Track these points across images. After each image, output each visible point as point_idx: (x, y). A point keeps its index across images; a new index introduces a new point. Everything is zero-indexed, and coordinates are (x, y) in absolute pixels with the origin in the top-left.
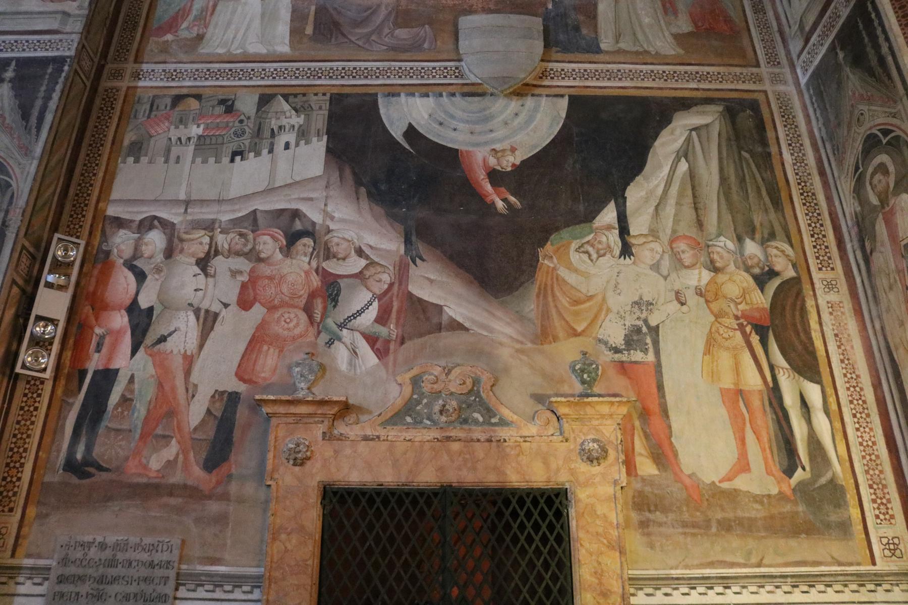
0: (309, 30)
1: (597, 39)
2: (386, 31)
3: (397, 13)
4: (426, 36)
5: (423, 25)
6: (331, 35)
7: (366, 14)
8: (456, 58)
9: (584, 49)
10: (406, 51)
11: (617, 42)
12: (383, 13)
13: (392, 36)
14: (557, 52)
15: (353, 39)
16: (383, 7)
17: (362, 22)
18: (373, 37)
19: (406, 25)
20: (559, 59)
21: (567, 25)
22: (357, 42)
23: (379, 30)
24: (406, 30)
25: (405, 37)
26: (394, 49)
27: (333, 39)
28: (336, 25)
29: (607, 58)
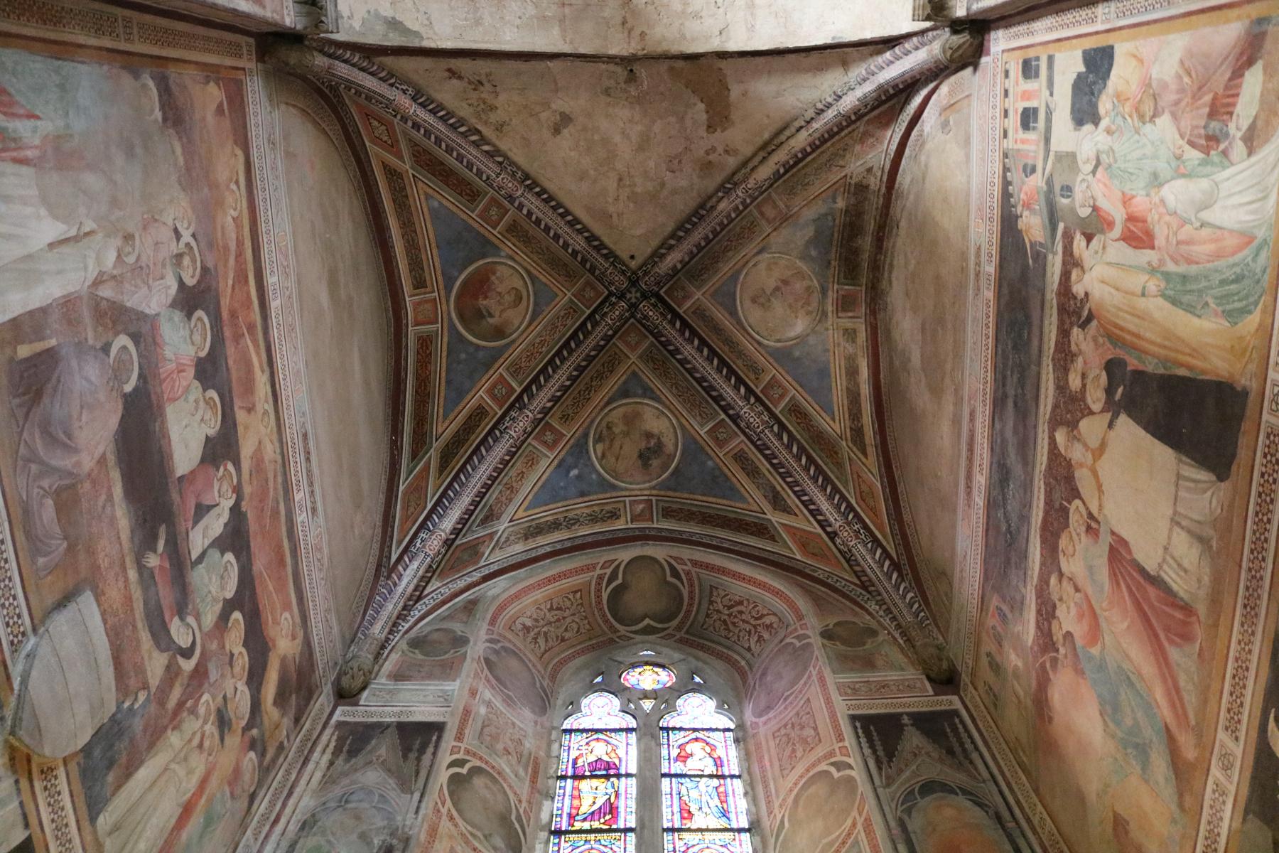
0: (24, 351)
1: (107, 801)
2: (45, 483)
3: (73, 485)
4: (53, 552)
5: (66, 538)
6: (24, 394)
7: (62, 436)
8: (36, 621)
9: (91, 797)
10: (28, 534)
11: (110, 834)
12: (65, 462)
13: (44, 496)
14: (78, 764)
15: (25, 435)
16: (74, 459)
17: (51, 435)
18: (34, 468)
19: (59, 509)
20: (71, 776)
21: (112, 746)
22: (22, 443)
23: (48, 470)
24: (54, 514)
25: (45, 521)
26: (27, 511)
27: (17, 401)
28: (38, 395)
29: (88, 838)
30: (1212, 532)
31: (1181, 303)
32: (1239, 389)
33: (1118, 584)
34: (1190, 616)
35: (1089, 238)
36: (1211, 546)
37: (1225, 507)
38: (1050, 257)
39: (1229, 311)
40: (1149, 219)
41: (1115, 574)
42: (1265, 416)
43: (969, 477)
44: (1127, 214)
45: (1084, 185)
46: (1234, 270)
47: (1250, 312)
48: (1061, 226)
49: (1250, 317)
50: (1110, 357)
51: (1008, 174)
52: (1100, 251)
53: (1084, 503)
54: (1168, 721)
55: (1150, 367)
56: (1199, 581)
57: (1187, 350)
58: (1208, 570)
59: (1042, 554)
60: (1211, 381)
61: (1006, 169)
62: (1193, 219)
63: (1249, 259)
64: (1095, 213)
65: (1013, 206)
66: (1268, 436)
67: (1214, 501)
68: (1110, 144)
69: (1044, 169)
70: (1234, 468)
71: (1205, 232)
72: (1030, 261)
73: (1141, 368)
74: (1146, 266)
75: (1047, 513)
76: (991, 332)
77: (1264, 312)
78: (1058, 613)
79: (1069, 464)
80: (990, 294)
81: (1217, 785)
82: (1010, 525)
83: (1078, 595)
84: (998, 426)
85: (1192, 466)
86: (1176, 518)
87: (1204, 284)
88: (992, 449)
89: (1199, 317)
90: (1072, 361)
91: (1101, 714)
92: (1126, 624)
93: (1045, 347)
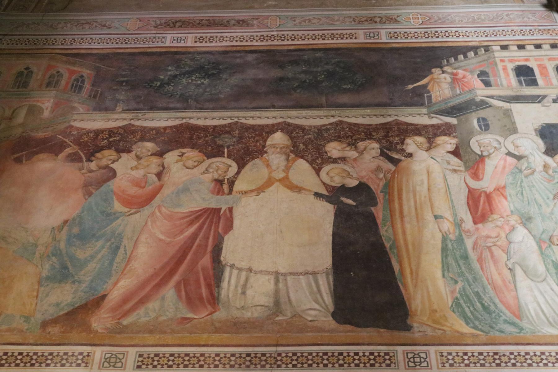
30: (289, 314)
31: (446, 256)
32: (409, 322)
33: (191, 223)
34: (210, 304)
35: (456, 153)
36: (278, 316)
37: (315, 324)
38: (424, 110)
39: (459, 303)
40: (495, 216)
41: (197, 218)
42: (400, 349)
43: (185, 24)
44: (491, 193)
45: (495, 144)
46: (491, 304)
47: (467, 324)
48: (453, 121)
49: (463, 323)
50: (372, 187)
51: (472, 53)
52: (451, 167)
53: (238, 173)
54: (109, 297)
55: (385, 232)
56: (243, 308)
57: (414, 268)
58: (256, 315)
59: (165, 128)
60: (401, 295)
61: (475, 49)
62: (512, 261)
63: (504, 317)
64: (478, 158)
65: (448, 61)
66: (387, 354)
67: (313, 313)
68: (537, 170)
69: (492, 97)
70: (348, 327)
71: (507, 273)
72: (410, 87)
73: (379, 221)
74: (459, 218)
75: (205, 129)
76: (329, 42)
77: (473, 335)
78: (124, 156)
79: (261, 152)
80: (361, 39)
81: (88, 356)
82: (168, 84)
83: (155, 178)
84: (250, 58)
85: (330, 288)
86: (281, 278)
87: (470, 277)
88: (225, 53)
89: (444, 276)
90: (349, 145)
91: (66, 222)
92: (162, 237)
93: (348, 112)
